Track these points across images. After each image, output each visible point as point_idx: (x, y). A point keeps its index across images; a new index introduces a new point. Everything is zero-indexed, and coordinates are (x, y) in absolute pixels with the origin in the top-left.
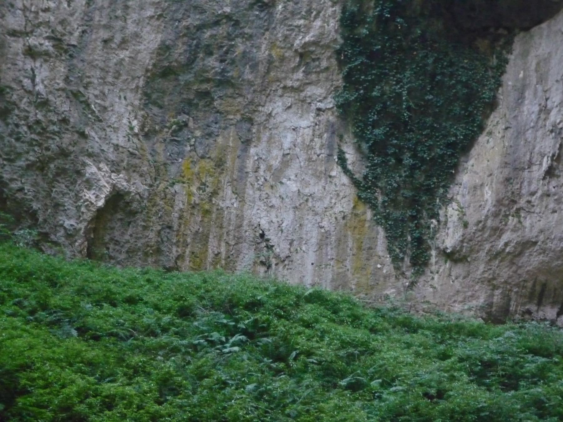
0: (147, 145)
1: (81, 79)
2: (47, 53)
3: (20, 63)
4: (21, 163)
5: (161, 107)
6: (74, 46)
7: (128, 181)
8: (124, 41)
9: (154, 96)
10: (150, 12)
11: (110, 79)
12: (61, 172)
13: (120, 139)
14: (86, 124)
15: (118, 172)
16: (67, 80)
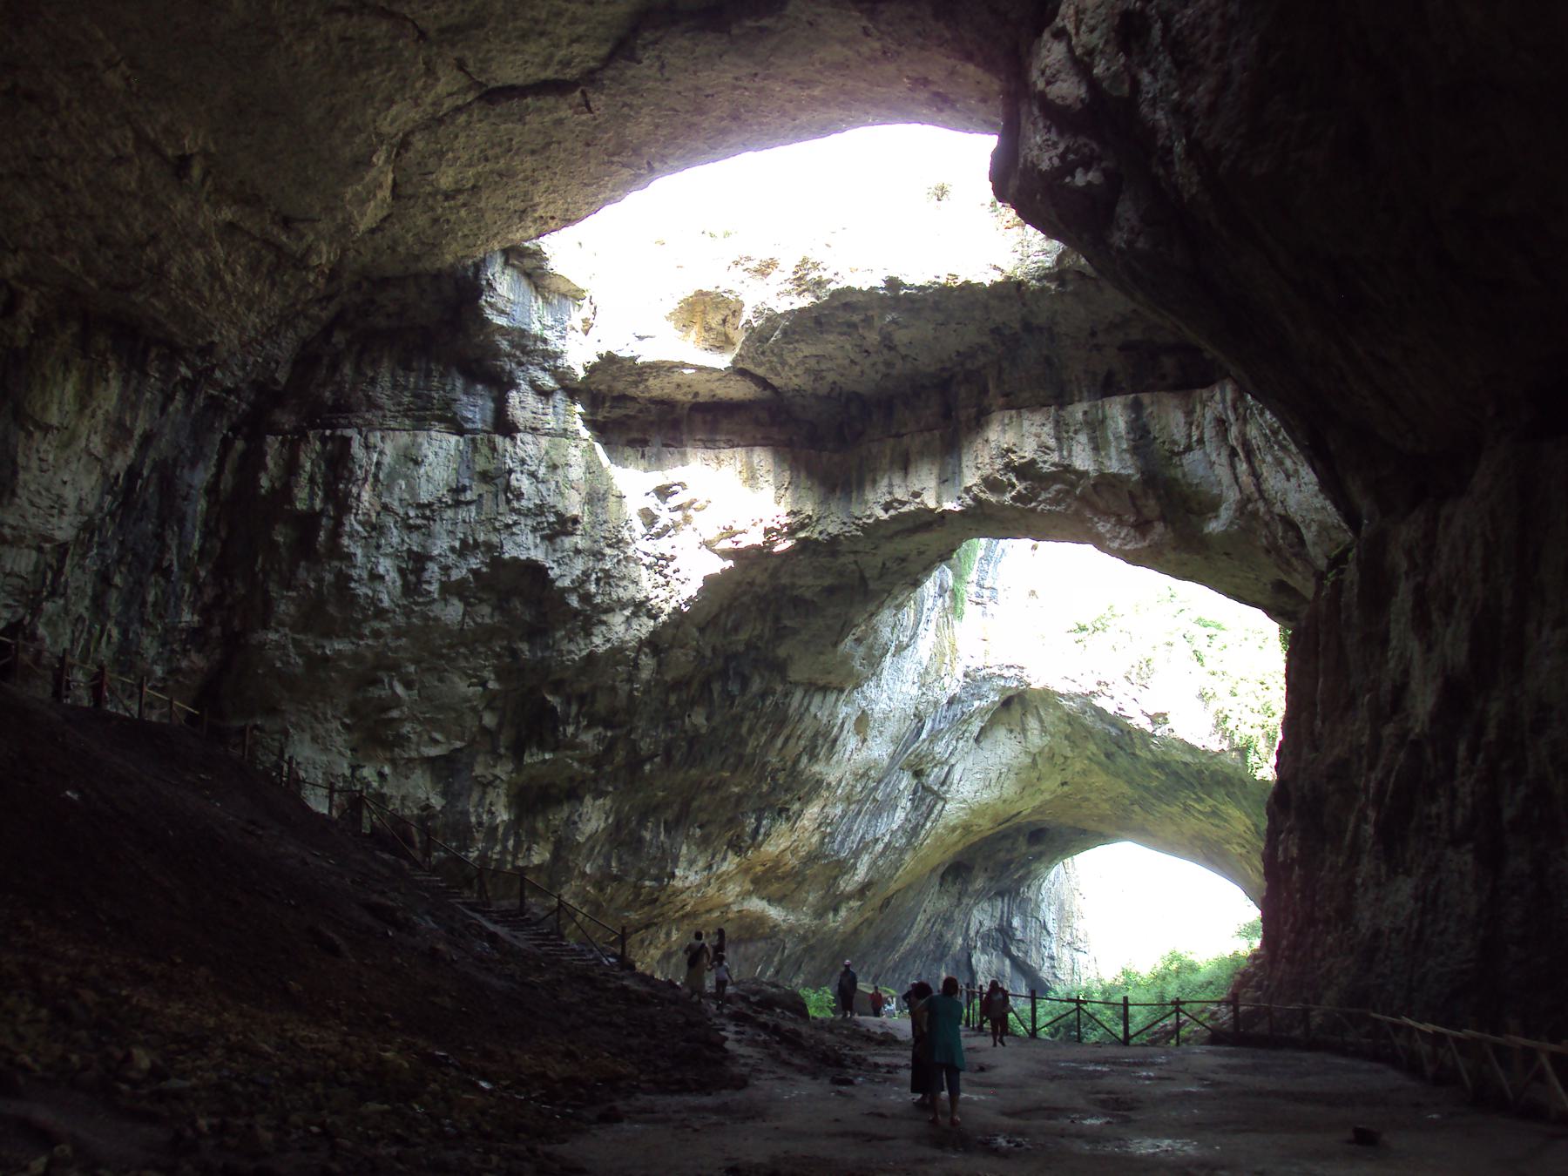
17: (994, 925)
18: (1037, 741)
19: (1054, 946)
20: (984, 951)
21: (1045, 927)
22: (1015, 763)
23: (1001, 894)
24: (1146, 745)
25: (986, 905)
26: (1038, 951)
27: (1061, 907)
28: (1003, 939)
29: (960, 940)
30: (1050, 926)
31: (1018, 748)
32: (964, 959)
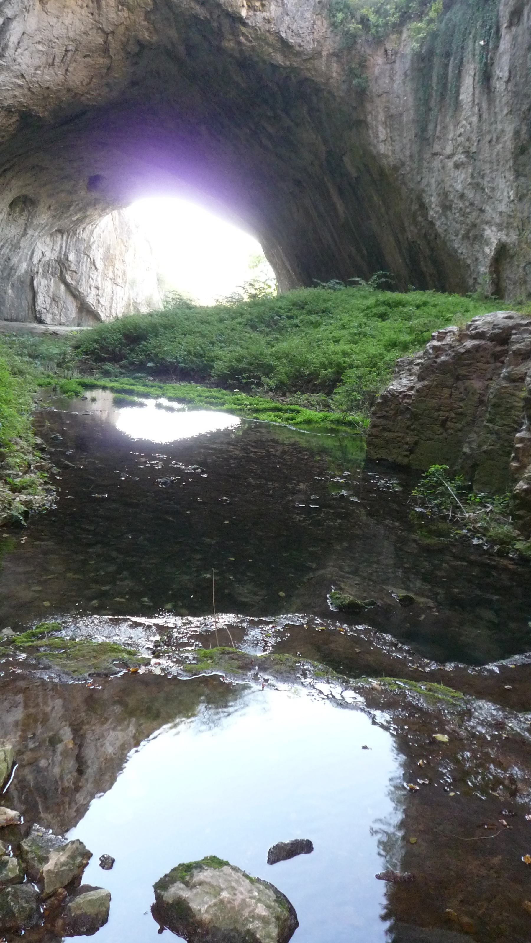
0: (519, 206)
1: (479, 173)
2: (463, 163)
3: (452, 174)
4: (460, 236)
5: (525, 176)
6: (475, 152)
7: (507, 235)
8: (498, 139)
9: (521, 170)
10: (505, 112)
11: (495, 167)
12: (475, 238)
13: (502, 207)
14: (484, 203)
15: (500, 230)
16: (472, 176)
17: (54, 256)
18: (112, 15)
19: (99, 279)
20: (44, 276)
21: (94, 264)
22: (84, 40)
23: (60, 231)
24: (235, 33)
25: (48, 240)
26: (88, 282)
27: (109, 249)
28: (61, 268)
29: (24, 266)
30: (99, 264)
31: (90, 20)
32: (28, 280)
